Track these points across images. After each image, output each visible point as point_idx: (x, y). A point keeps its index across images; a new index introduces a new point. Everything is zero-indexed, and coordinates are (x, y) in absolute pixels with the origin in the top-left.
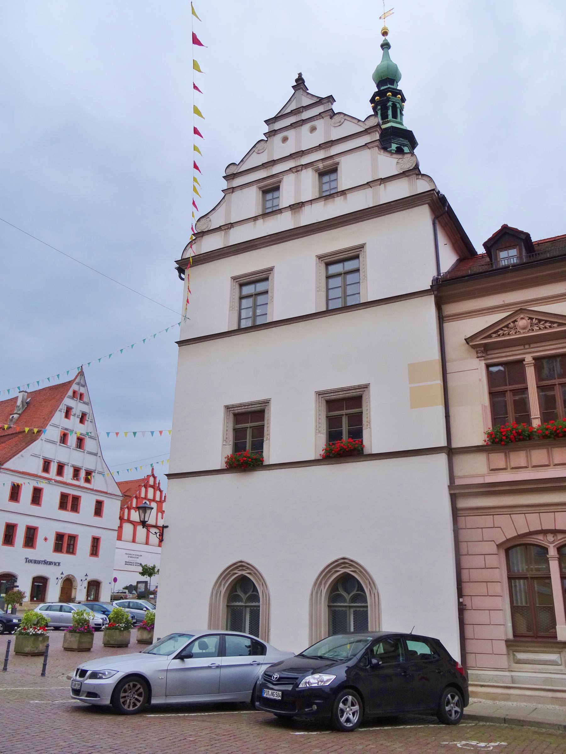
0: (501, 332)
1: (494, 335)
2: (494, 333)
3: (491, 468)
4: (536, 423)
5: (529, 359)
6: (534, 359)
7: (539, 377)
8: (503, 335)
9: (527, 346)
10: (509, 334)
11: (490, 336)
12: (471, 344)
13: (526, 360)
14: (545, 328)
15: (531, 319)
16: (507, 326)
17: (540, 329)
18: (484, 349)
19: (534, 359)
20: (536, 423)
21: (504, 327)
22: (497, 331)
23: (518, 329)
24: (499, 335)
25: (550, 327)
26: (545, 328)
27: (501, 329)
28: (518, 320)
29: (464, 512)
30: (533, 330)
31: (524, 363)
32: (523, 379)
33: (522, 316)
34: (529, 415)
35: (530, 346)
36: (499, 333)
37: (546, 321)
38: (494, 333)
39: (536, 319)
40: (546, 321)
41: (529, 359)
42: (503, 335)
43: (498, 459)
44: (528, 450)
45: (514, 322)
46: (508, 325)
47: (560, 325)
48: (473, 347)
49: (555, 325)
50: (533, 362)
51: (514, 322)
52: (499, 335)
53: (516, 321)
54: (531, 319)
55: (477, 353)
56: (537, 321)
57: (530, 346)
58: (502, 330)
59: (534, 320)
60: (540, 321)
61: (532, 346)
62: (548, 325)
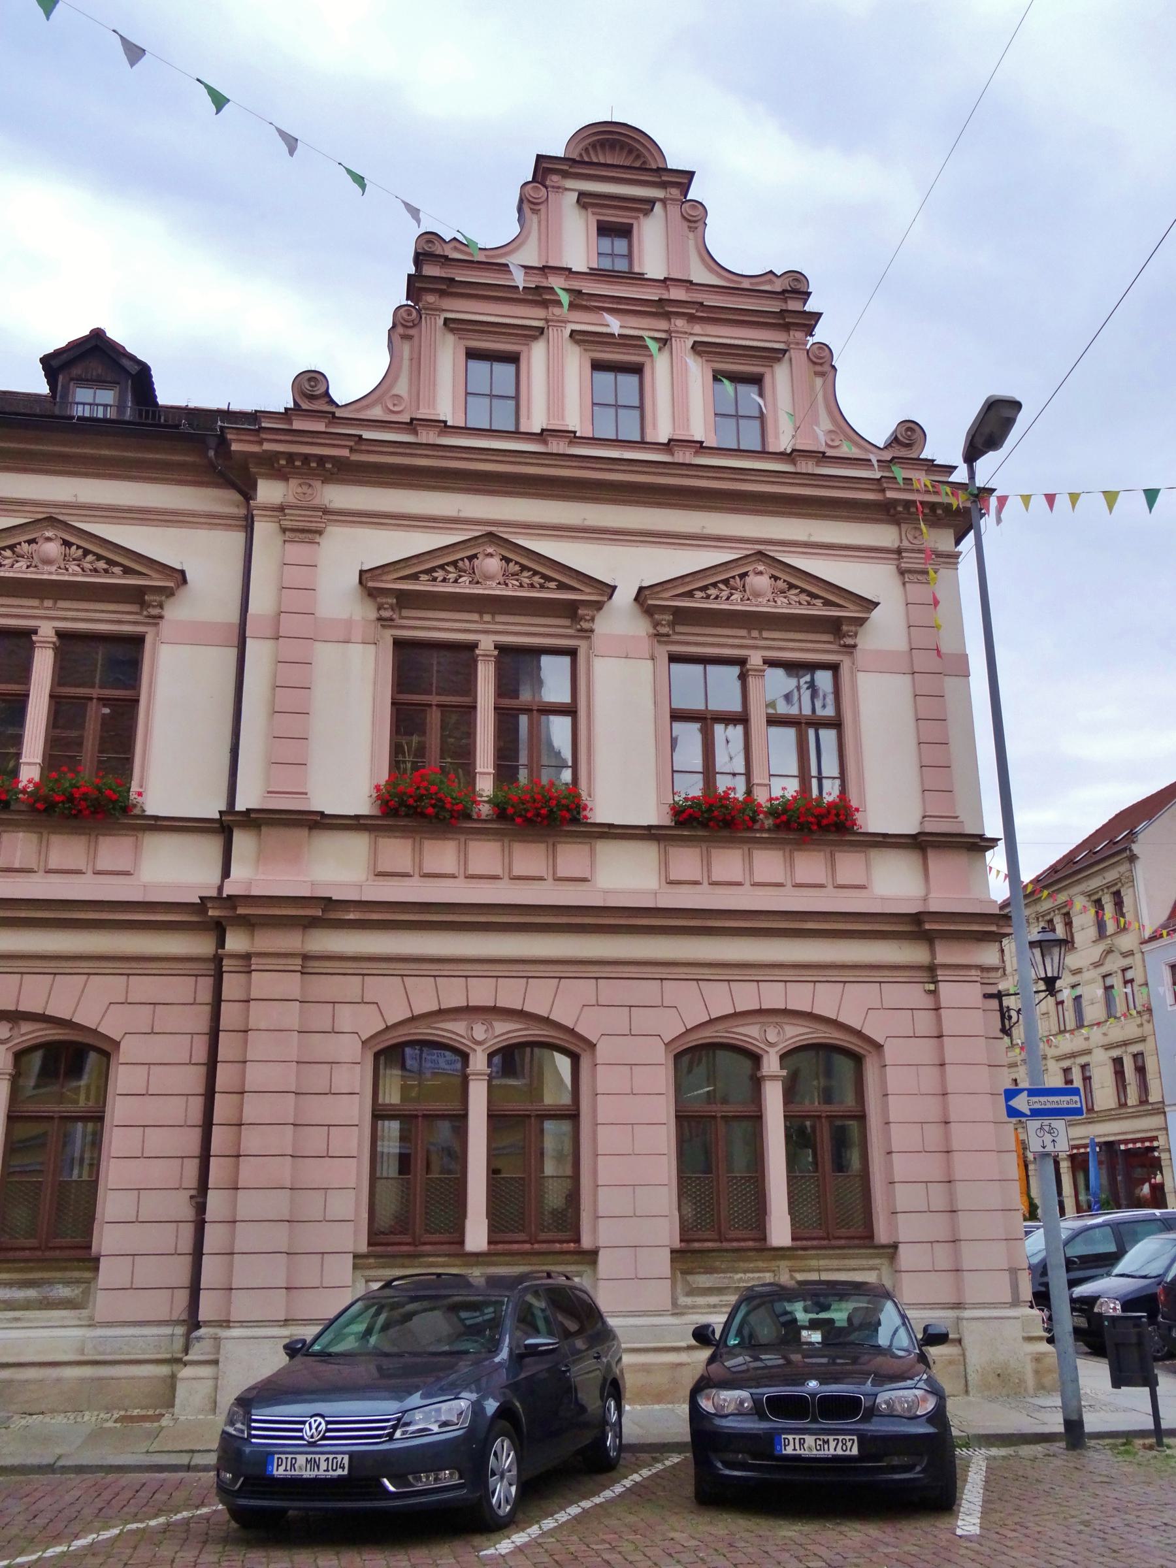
0: (440, 574)
1: (424, 577)
3: (380, 869)
4: (485, 785)
5: (486, 644)
8: (444, 580)
9: (487, 618)
10: (456, 581)
11: (415, 577)
12: (370, 584)
13: (482, 646)
14: (532, 586)
16: (454, 563)
17: (521, 586)
18: (397, 603)
20: (485, 785)
21: (447, 564)
22: (433, 570)
24: (435, 579)
25: (542, 586)
26: (532, 586)
27: (442, 567)
28: (480, 556)
29: (316, 964)
30: (507, 585)
31: (477, 652)
32: (468, 686)
33: (490, 550)
34: (473, 764)
36: (435, 574)
39: (517, 563)
40: (536, 573)
41: (486, 644)
43: (397, 851)
44: (418, 839)
45: (471, 558)
47: (562, 586)
48: (372, 593)
49: (552, 585)
51: (471, 558)
52: (435, 579)
53: (475, 556)
55: (379, 609)
57: (493, 618)
59: (511, 564)
60: (524, 568)
61: (499, 618)
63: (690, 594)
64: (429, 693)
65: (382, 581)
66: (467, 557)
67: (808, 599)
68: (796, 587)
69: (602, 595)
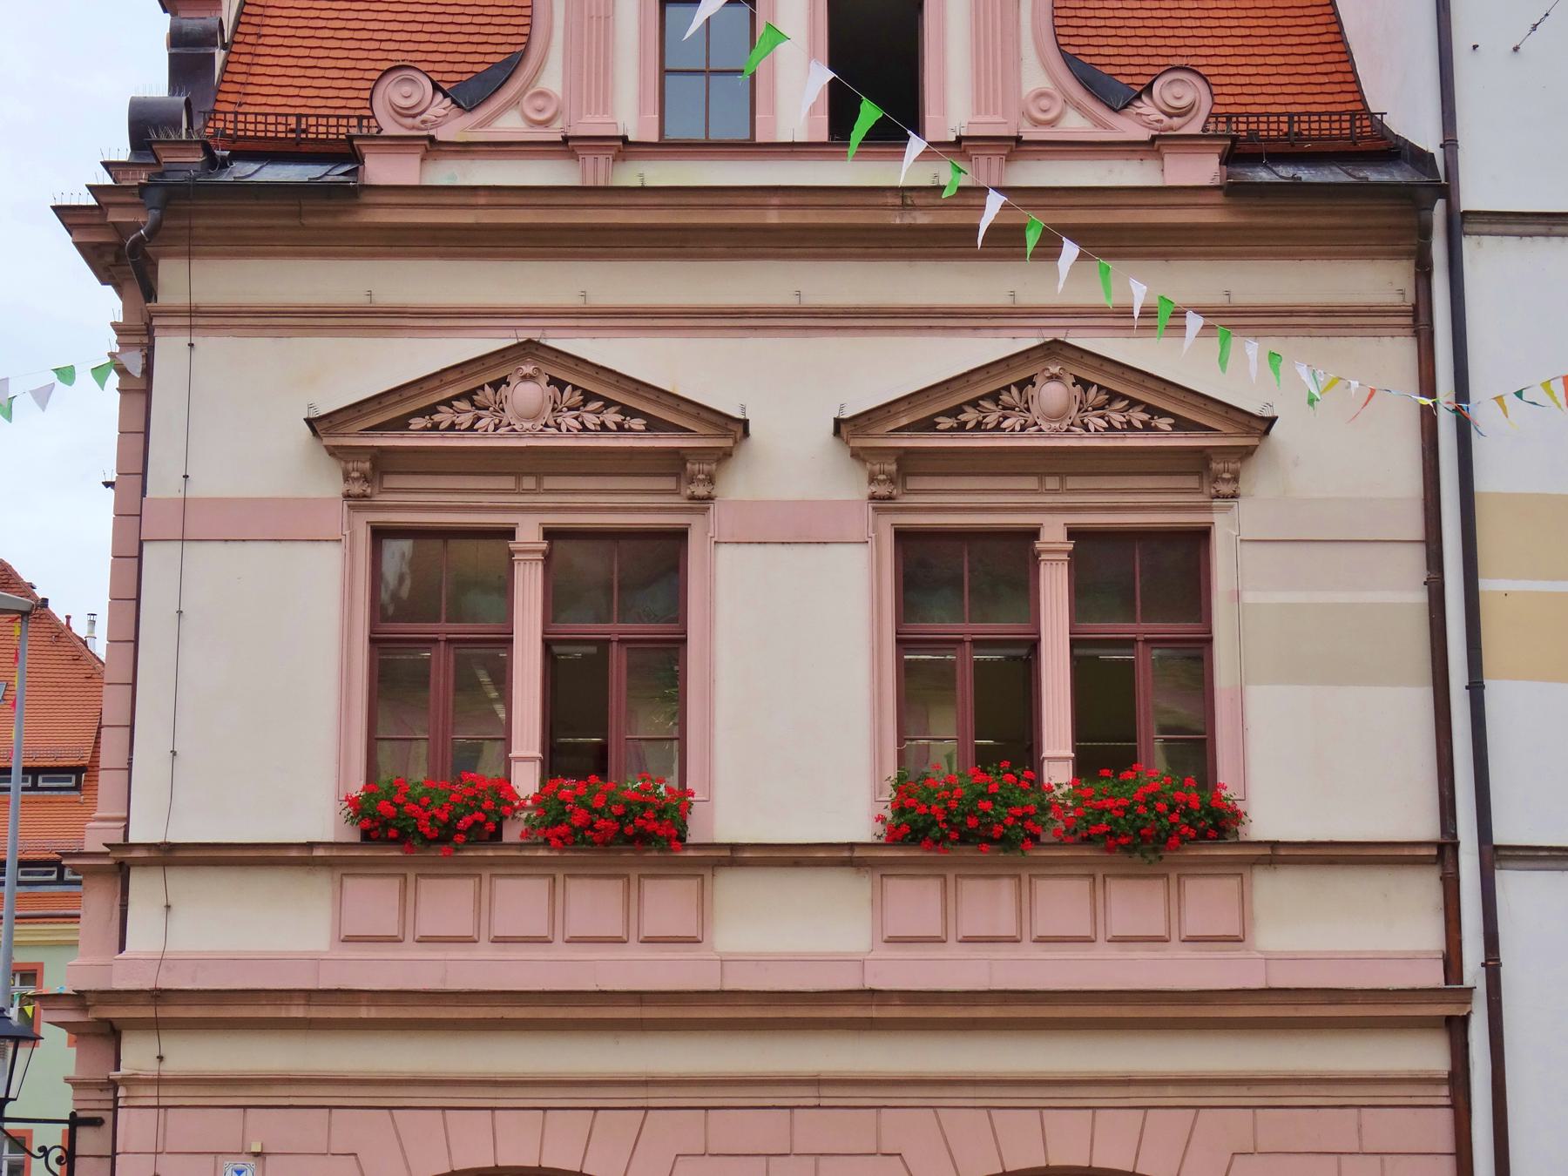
2: (420, 413)
6: (550, 534)
7: (556, 602)
8: (452, 427)
13: (519, 536)
14: (604, 427)
15: (561, 385)
18: (374, 468)
19: (550, 534)
21: (458, 398)
22: (431, 410)
23: (508, 416)
25: (620, 427)
31: (512, 546)
33: (528, 369)
35: (539, 483)
36: (437, 418)
37: (609, 403)
38: (420, 413)
42: (452, 427)
45: (496, 385)
46: (474, 391)
47: (654, 425)
50: (544, 546)
51: (496, 385)
54: (561, 385)
56: (577, 397)
57: (539, 483)
58: (451, 406)
61: (549, 483)
62: (611, 417)
63: (928, 425)
64: (437, 619)
65: (344, 435)
66: (490, 384)
67: (1146, 417)
68: (1124, 397)
69: (725, 436)
